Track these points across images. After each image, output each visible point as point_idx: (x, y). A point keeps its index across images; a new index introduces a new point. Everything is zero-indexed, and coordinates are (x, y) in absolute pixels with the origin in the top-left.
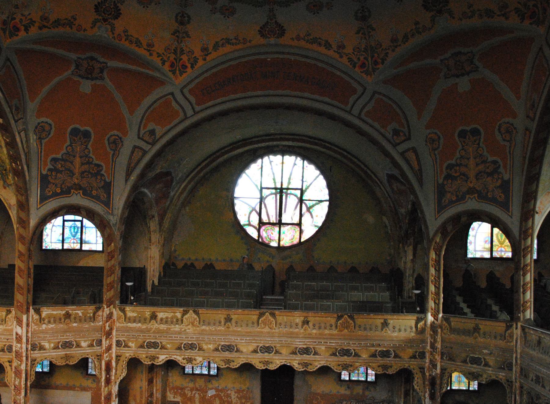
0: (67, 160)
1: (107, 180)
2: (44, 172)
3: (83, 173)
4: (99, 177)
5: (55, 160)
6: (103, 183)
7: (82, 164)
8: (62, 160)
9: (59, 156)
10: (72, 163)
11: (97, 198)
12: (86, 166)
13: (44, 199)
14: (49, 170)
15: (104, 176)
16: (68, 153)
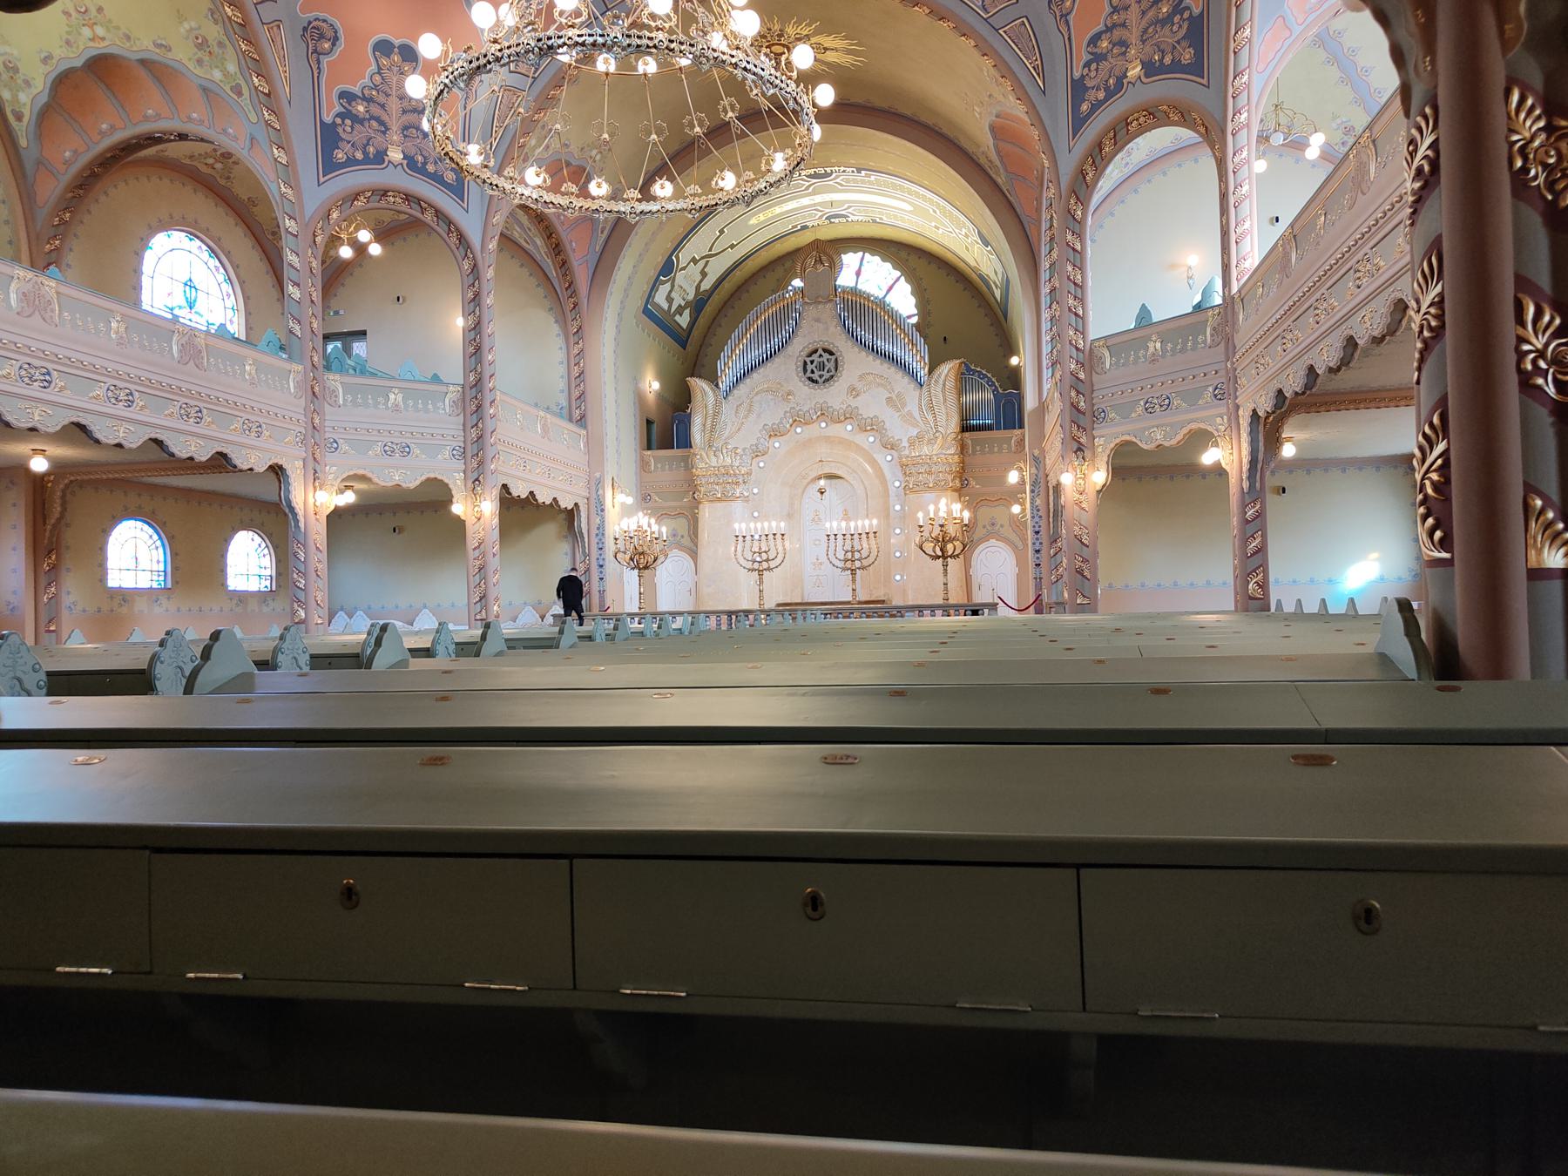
0: (1114, 26)
1: (1196, 12)
2: (1077, 75)
3: (1145, 31)
4: (1177, 19)
5: (1094, 40)
6: (1185, 26)
7: (1144, 13)
8: (1109, 29)
9: (1101, 27)
10: (1123, 25)
11: (1176, 67)
12: (1151, 14)
13: (1078, 123)
14: (1087, 65)
15: (1187, 8)
16: (1115, 10)
